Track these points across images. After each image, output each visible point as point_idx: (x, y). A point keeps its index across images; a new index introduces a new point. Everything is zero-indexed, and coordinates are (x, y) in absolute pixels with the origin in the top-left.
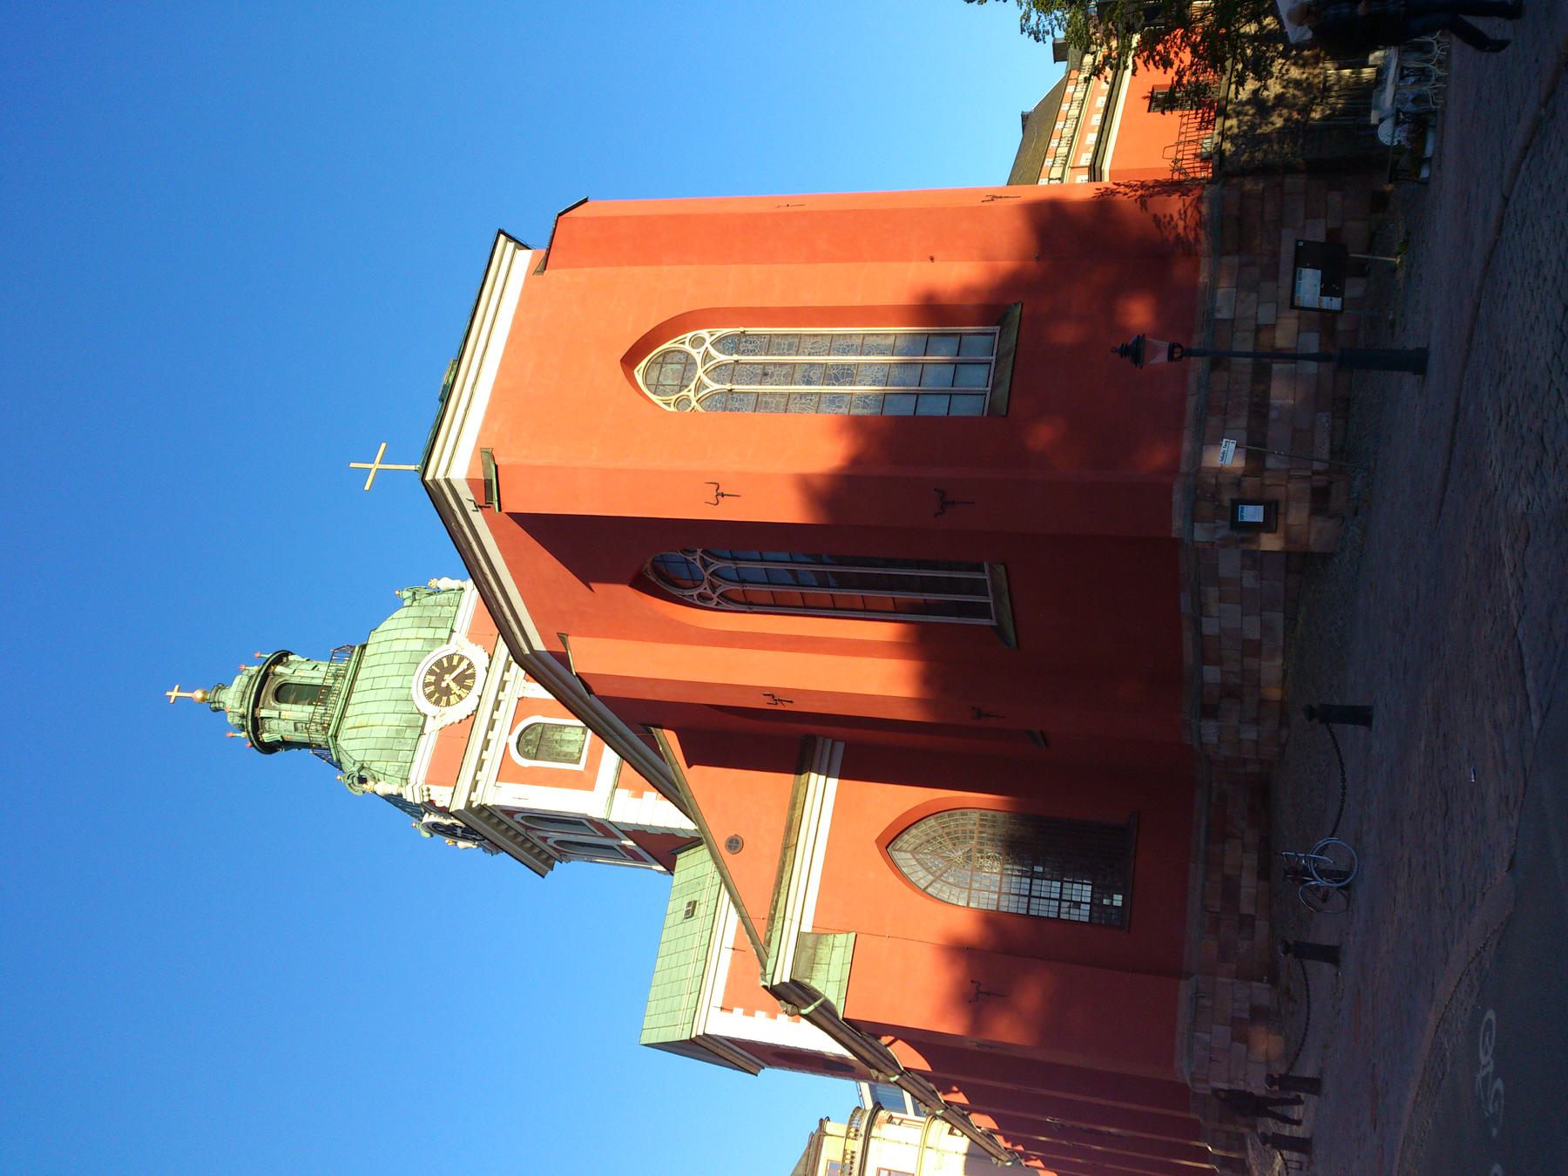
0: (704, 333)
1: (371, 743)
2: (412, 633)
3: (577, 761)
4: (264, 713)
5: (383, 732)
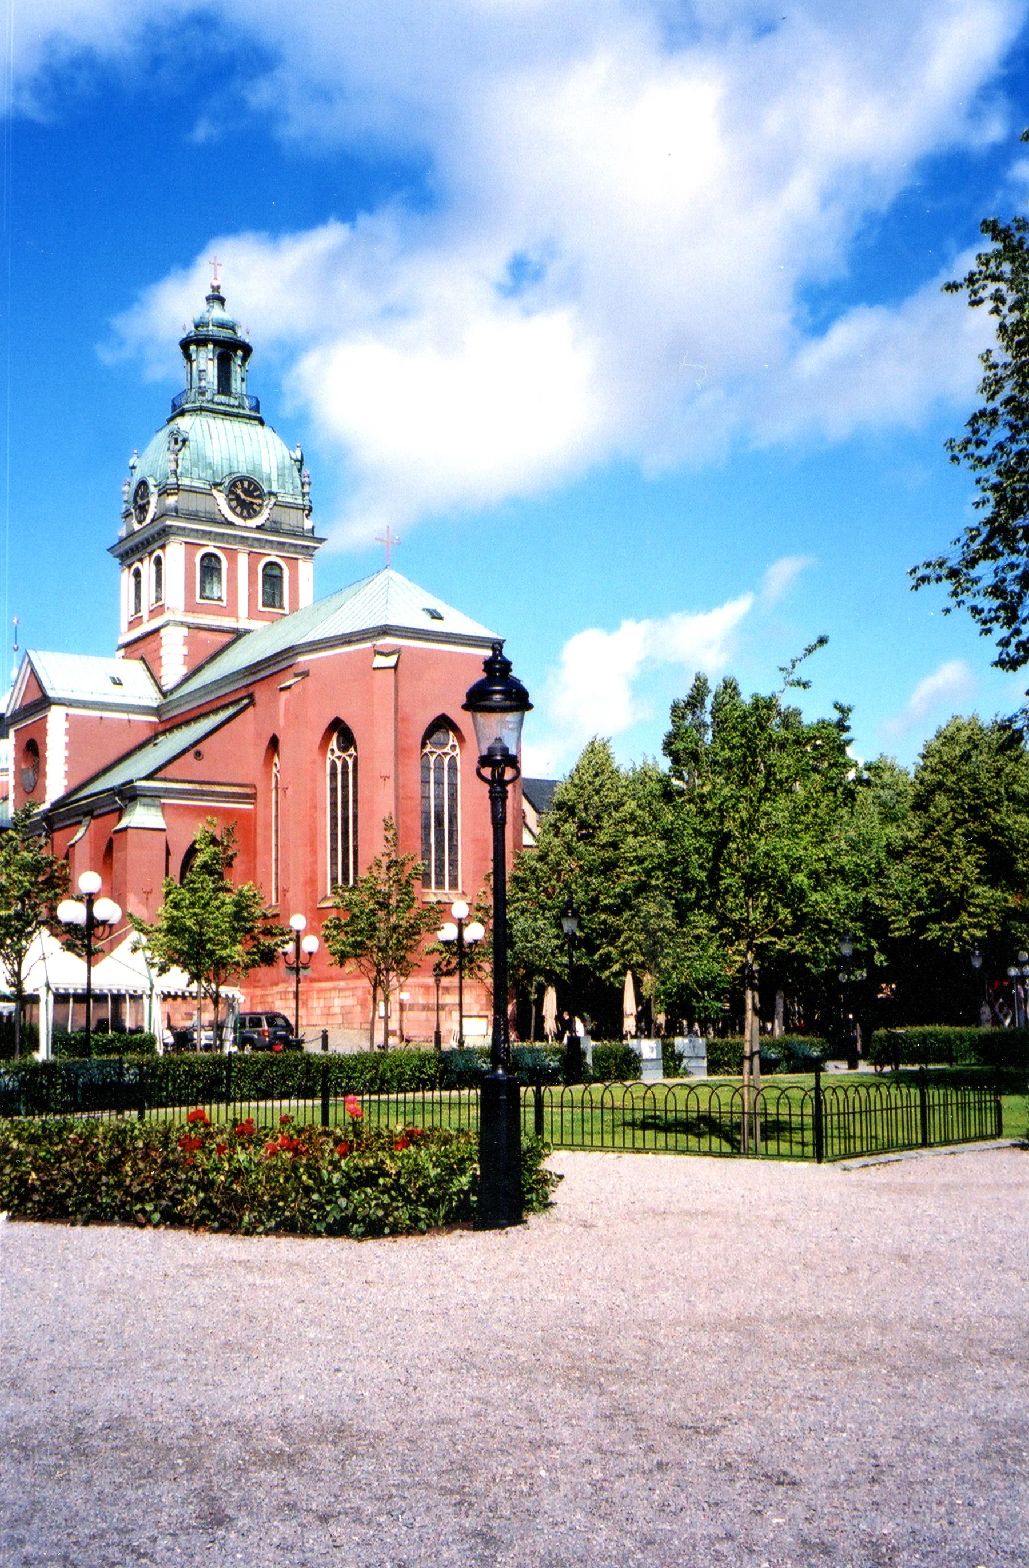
0: (458, 750)
1: (201, 445)
3: (202, 597)
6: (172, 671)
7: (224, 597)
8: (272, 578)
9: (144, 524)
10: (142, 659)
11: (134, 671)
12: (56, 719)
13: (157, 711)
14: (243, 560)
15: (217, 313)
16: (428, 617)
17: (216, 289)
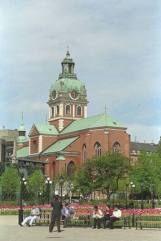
2: (80, 87)
4: (67, 64)
5: (68, 86)
6: (61, 128)
7: (70, 113)
8: (79, 109)
9: (55, 99)
10: (54, 125)
11: (53, 127)
12: (41, 137)
13: (58, 136)
14: (74, 106)
15: (69, 57)
16: (114, 124)
17: (68, 52)
